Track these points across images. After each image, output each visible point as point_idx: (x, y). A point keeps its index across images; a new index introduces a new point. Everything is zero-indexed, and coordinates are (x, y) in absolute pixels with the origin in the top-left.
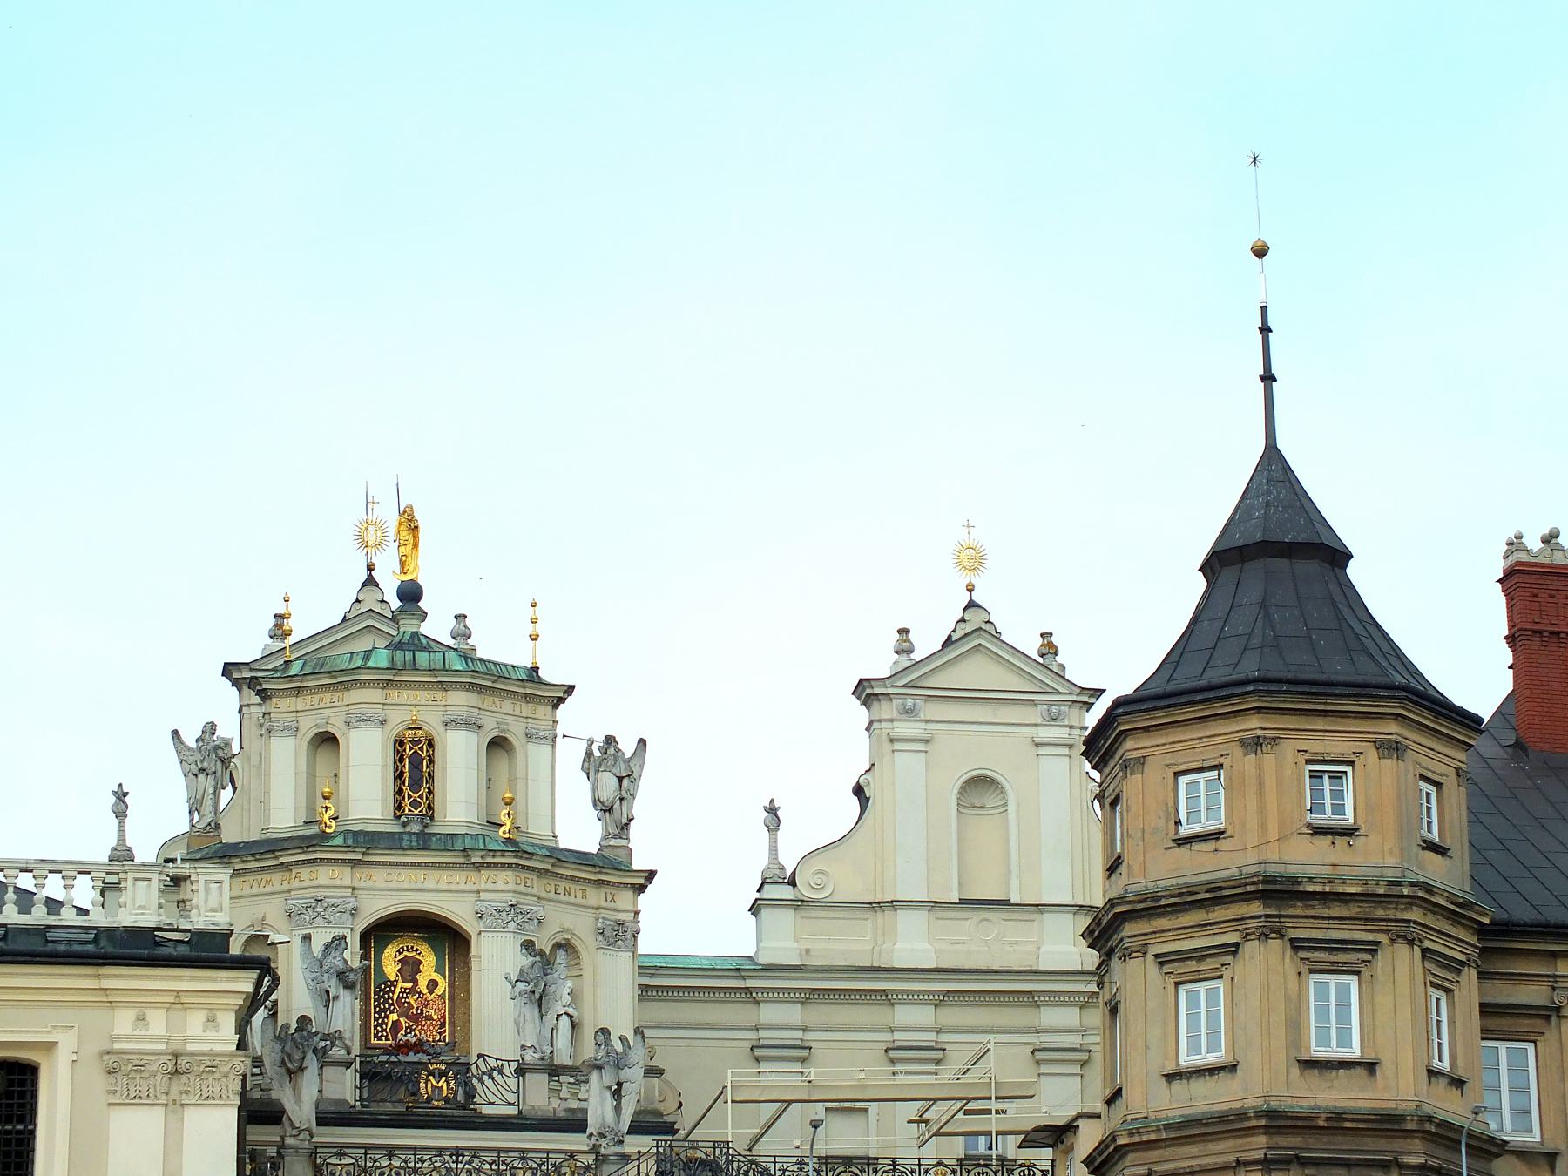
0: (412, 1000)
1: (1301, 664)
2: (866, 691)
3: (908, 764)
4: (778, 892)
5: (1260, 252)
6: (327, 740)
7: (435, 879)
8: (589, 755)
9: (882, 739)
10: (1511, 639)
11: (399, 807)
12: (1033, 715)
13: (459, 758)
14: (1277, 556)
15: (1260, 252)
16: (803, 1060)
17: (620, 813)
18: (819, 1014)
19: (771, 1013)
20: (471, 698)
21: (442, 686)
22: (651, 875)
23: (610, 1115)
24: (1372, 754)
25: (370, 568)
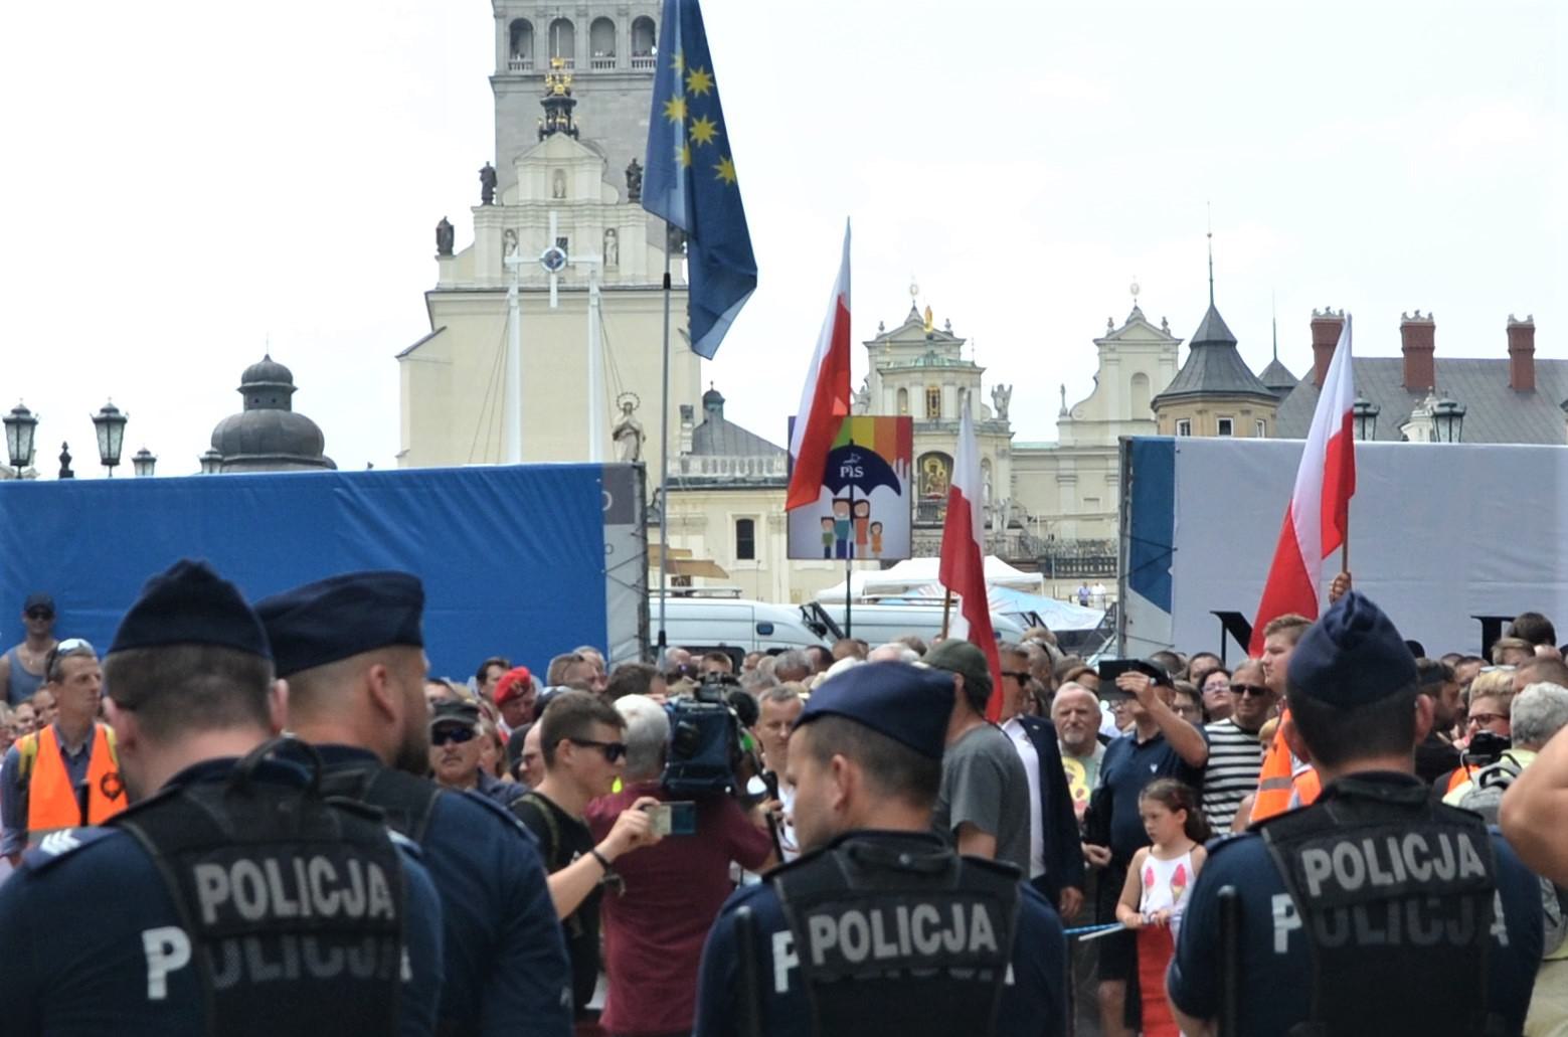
0: (935, 479)
1: (1216, 385)
2: (1097, 342)
3: (1112, 369)
4: (1068, 420)
5: (1210, 236)
6: (903, 391)
7: (940, 440)
8: (993, 392)
9: (1104, 361)
10: (1314, 346)
11: (928, 414)
12: (1160, 349)
13: (949, 396)
14: (1216, 343)
15: (1210, 236)
16: (1074, 481)
17: (1004, 411)
18: (1081, 463)
19: (1063, 464)
20: (953, 375)
21: (943, 371)
22: (1013, 433)
23: (1000, 526)
24: (1239, 414)
25: (914, 302)
